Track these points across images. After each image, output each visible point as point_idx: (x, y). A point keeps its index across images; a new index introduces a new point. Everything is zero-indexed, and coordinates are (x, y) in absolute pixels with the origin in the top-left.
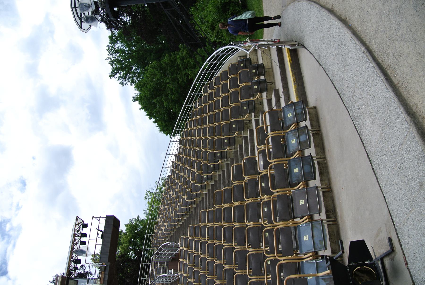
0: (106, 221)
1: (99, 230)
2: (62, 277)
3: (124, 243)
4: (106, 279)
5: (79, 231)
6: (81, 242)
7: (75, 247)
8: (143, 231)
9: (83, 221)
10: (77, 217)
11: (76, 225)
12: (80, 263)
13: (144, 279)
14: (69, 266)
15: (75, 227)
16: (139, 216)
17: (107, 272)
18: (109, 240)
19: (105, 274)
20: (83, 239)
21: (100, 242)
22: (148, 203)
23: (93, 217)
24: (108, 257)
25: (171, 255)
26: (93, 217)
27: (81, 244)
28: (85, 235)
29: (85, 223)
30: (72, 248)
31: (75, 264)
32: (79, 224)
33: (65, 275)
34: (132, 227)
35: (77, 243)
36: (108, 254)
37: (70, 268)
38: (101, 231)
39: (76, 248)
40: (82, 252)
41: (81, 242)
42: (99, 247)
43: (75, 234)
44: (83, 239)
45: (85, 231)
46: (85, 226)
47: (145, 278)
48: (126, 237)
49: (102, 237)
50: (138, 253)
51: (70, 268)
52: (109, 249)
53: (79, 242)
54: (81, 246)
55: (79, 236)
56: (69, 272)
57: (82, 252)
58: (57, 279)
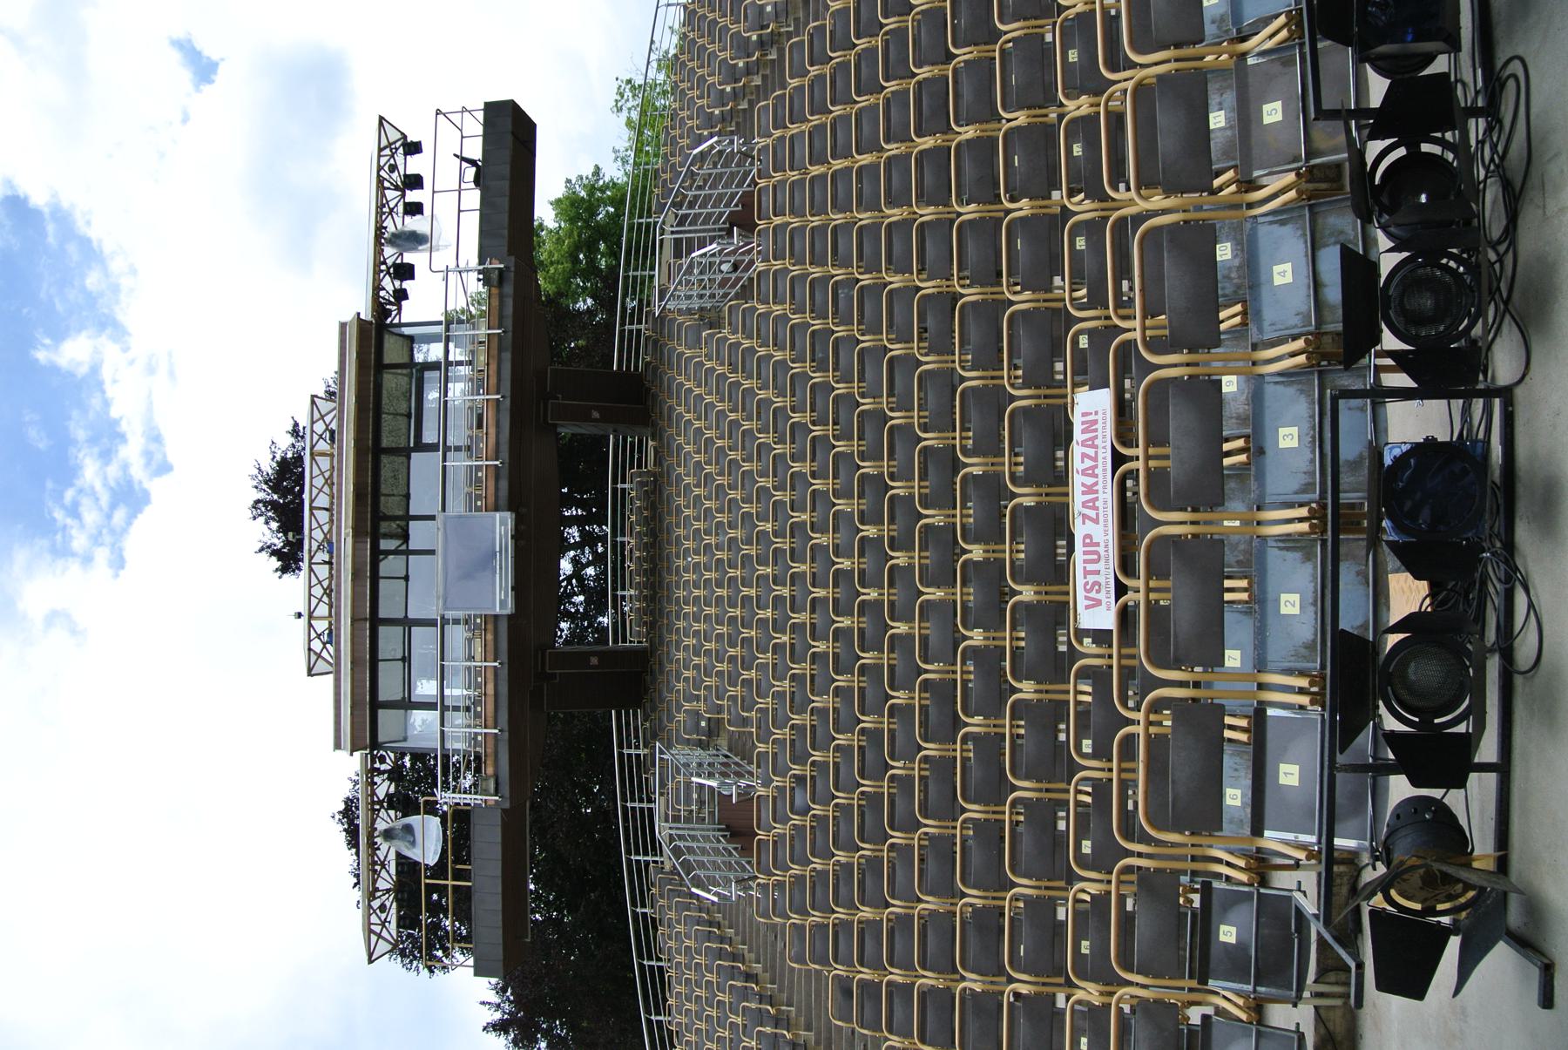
0: (487, 124)
1: (463, 159)
2: (361, 323)
3: (552, 263)
4: (509, 310)
5: (393, 168)
6: (406, 204)
7: (388, 223)
8: (615, 218)
9: (405, 137)
10: (381, 119)
11: (380, 150)
12: (412, 277)
13: (634, 327)
14: (377, 288)
15: (379, 156)
16: (597, 168)
17: (509, 289)
18: (506, 184)
19: (501, 297)
20: (412, 196)
21: (473, 198)
22: (629, 123)
23: (438, 112)
24: (505, 242)
25: (727, 205)
26: (438, 112)
27: (406, 154)
28: (415, 182)
29: (411, 138)
30: (380, 229)
31: (397, 283)
32: (390, 144)
33: (366, 315)
34: (576, 207)
35: (391, 210)
36: (506, 232)
37: (382, 293)
38: (473, 162)
39: (391, 229)
40: (415, 240)
41: (406, 204)
42: (472, 223)
43: (380, 180)
44: (412, 196)
45: (415, 165)
46: (413, 148)
47: (640, 322)
48: (559, 241)
49: (477, 181)
50: (606, 301)
51: (382, 293)
52: (506, 217)
53: (401, 208)
54: (408, 218)
55: (397, 188)
56: (381, 310)
57: (415, 240)
58: (342, 389)
